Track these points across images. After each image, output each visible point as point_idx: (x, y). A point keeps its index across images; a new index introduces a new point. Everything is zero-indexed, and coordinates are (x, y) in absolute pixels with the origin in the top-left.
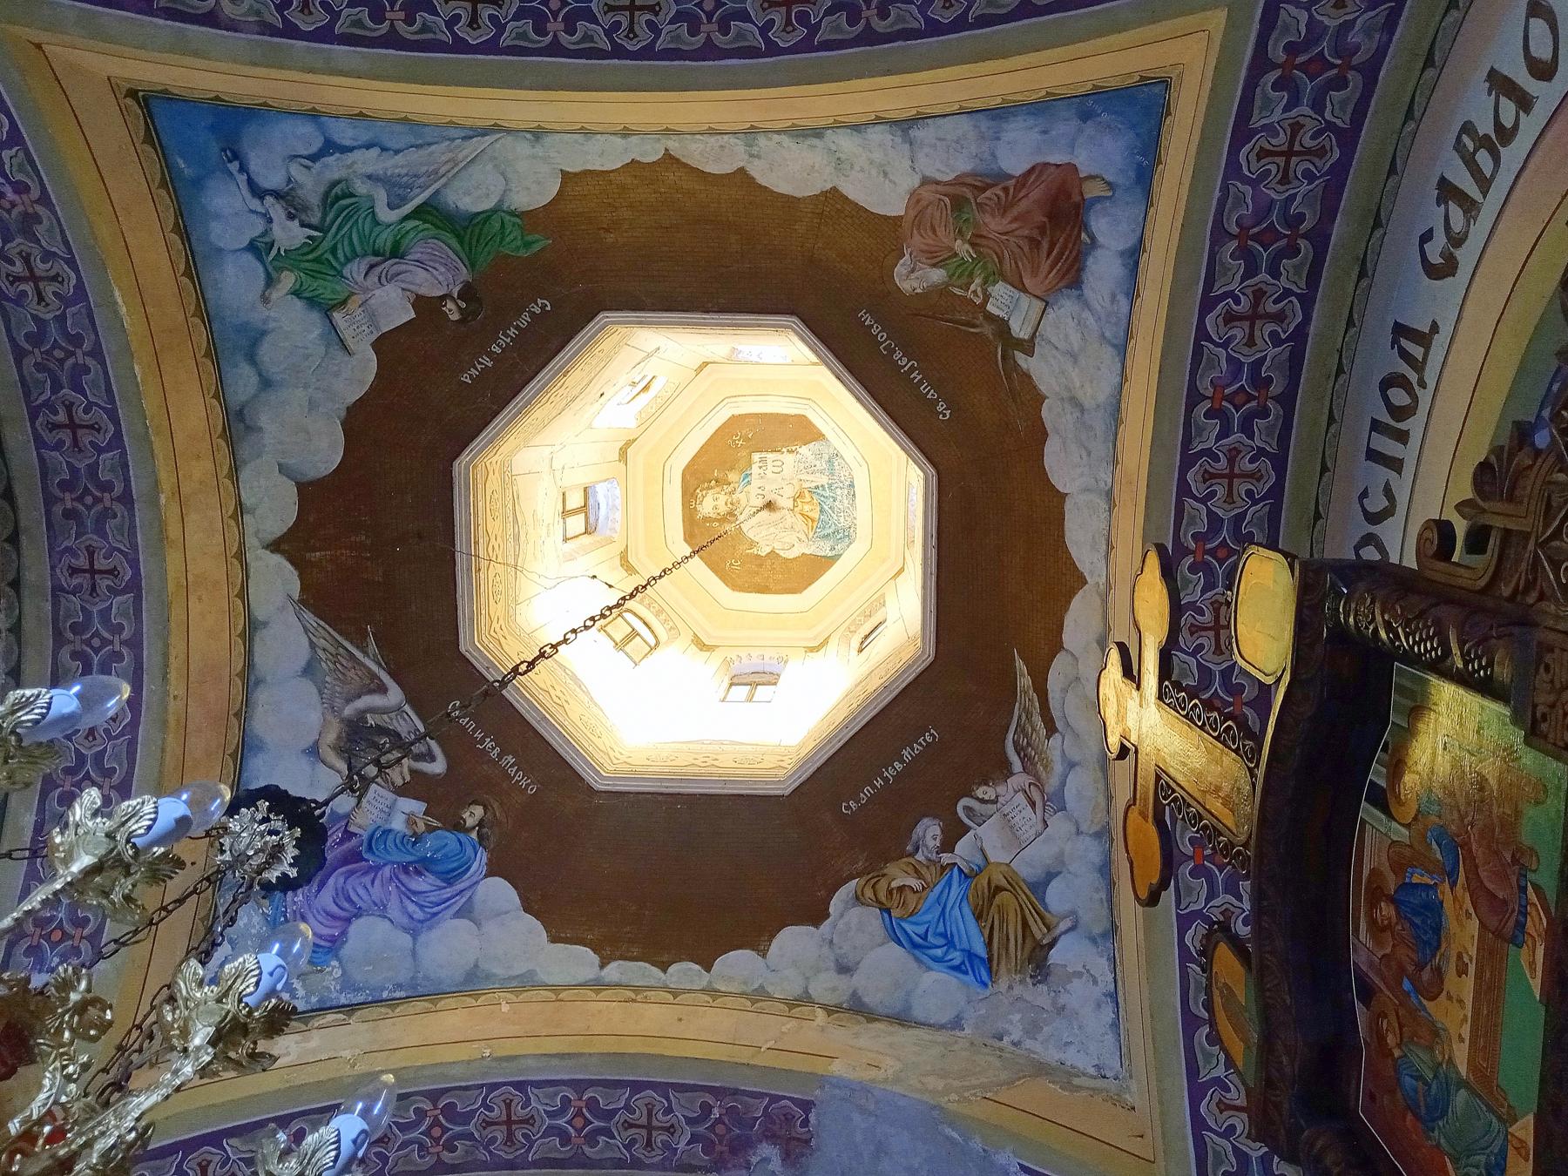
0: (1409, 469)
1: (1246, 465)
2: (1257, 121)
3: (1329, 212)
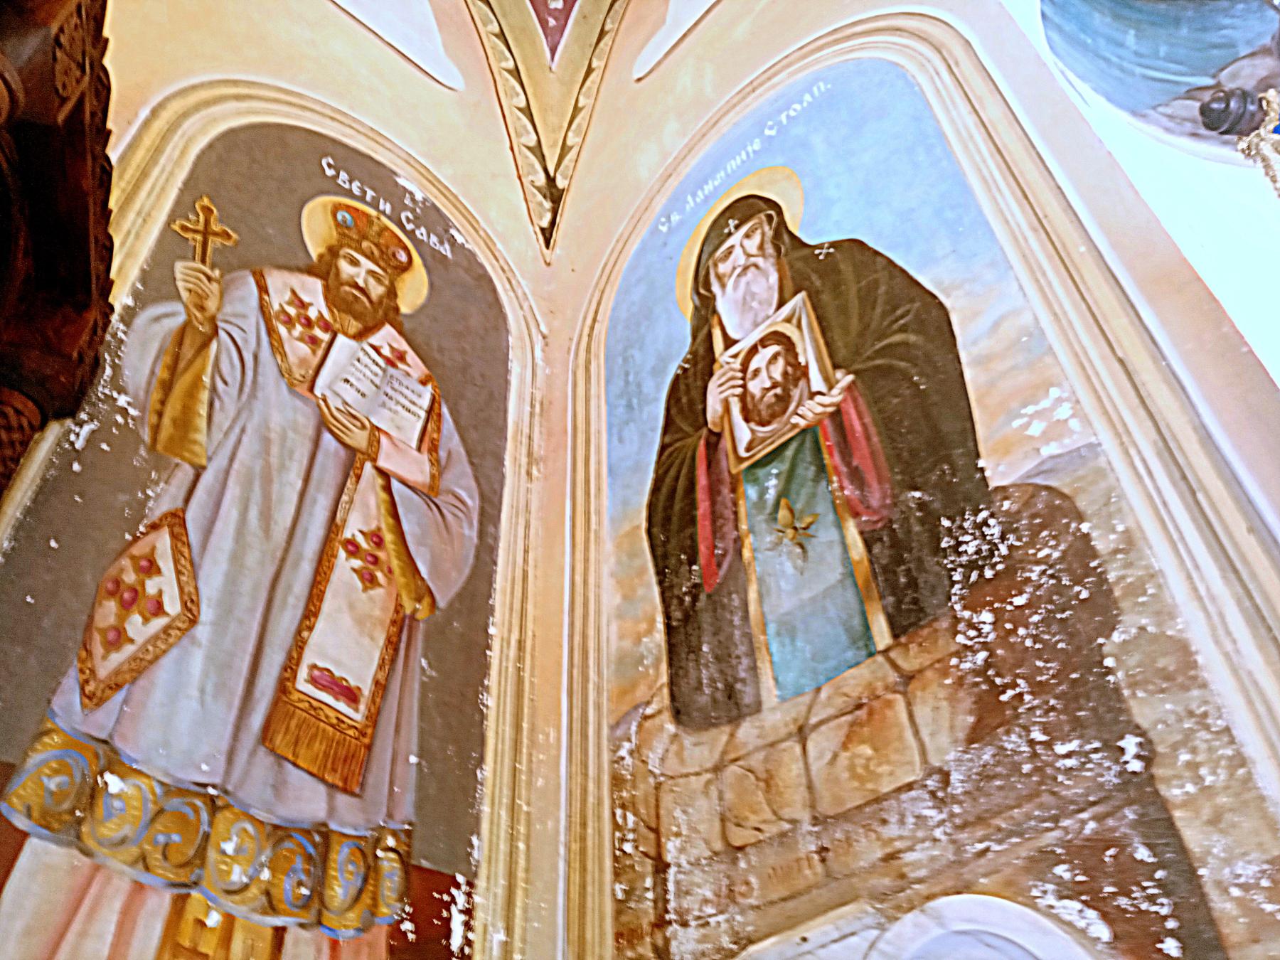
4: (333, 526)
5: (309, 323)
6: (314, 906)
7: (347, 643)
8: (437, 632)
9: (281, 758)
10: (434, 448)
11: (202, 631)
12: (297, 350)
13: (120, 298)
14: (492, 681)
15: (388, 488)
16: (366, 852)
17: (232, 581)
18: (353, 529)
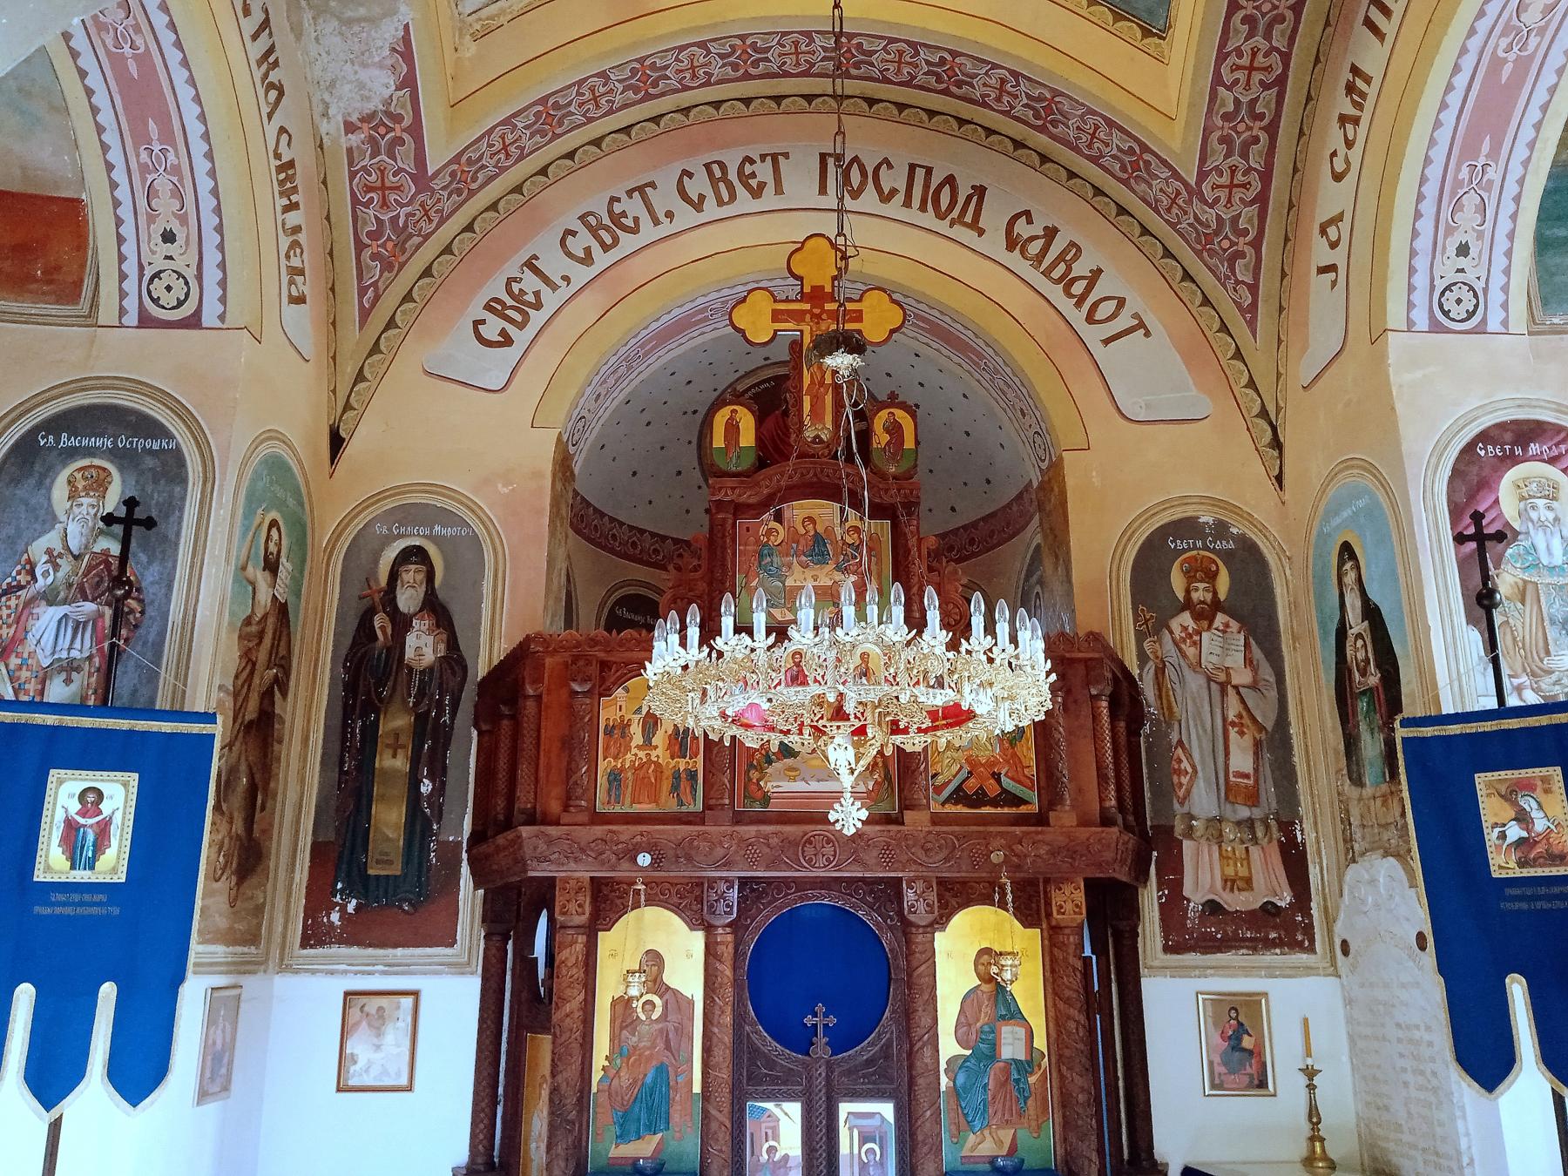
0: (904, 214)
3: (1053, 137)
4: (1224, 719)
5: (1190, 636)
6: (1255, 840)
7: (1242, 760)
8: (1271, 739)
11: (1200, 774)
12: (1191, 652)
13: (1136, 672)
15: (1238, 693)
16: (1265, 821)
18: (1231, 716)
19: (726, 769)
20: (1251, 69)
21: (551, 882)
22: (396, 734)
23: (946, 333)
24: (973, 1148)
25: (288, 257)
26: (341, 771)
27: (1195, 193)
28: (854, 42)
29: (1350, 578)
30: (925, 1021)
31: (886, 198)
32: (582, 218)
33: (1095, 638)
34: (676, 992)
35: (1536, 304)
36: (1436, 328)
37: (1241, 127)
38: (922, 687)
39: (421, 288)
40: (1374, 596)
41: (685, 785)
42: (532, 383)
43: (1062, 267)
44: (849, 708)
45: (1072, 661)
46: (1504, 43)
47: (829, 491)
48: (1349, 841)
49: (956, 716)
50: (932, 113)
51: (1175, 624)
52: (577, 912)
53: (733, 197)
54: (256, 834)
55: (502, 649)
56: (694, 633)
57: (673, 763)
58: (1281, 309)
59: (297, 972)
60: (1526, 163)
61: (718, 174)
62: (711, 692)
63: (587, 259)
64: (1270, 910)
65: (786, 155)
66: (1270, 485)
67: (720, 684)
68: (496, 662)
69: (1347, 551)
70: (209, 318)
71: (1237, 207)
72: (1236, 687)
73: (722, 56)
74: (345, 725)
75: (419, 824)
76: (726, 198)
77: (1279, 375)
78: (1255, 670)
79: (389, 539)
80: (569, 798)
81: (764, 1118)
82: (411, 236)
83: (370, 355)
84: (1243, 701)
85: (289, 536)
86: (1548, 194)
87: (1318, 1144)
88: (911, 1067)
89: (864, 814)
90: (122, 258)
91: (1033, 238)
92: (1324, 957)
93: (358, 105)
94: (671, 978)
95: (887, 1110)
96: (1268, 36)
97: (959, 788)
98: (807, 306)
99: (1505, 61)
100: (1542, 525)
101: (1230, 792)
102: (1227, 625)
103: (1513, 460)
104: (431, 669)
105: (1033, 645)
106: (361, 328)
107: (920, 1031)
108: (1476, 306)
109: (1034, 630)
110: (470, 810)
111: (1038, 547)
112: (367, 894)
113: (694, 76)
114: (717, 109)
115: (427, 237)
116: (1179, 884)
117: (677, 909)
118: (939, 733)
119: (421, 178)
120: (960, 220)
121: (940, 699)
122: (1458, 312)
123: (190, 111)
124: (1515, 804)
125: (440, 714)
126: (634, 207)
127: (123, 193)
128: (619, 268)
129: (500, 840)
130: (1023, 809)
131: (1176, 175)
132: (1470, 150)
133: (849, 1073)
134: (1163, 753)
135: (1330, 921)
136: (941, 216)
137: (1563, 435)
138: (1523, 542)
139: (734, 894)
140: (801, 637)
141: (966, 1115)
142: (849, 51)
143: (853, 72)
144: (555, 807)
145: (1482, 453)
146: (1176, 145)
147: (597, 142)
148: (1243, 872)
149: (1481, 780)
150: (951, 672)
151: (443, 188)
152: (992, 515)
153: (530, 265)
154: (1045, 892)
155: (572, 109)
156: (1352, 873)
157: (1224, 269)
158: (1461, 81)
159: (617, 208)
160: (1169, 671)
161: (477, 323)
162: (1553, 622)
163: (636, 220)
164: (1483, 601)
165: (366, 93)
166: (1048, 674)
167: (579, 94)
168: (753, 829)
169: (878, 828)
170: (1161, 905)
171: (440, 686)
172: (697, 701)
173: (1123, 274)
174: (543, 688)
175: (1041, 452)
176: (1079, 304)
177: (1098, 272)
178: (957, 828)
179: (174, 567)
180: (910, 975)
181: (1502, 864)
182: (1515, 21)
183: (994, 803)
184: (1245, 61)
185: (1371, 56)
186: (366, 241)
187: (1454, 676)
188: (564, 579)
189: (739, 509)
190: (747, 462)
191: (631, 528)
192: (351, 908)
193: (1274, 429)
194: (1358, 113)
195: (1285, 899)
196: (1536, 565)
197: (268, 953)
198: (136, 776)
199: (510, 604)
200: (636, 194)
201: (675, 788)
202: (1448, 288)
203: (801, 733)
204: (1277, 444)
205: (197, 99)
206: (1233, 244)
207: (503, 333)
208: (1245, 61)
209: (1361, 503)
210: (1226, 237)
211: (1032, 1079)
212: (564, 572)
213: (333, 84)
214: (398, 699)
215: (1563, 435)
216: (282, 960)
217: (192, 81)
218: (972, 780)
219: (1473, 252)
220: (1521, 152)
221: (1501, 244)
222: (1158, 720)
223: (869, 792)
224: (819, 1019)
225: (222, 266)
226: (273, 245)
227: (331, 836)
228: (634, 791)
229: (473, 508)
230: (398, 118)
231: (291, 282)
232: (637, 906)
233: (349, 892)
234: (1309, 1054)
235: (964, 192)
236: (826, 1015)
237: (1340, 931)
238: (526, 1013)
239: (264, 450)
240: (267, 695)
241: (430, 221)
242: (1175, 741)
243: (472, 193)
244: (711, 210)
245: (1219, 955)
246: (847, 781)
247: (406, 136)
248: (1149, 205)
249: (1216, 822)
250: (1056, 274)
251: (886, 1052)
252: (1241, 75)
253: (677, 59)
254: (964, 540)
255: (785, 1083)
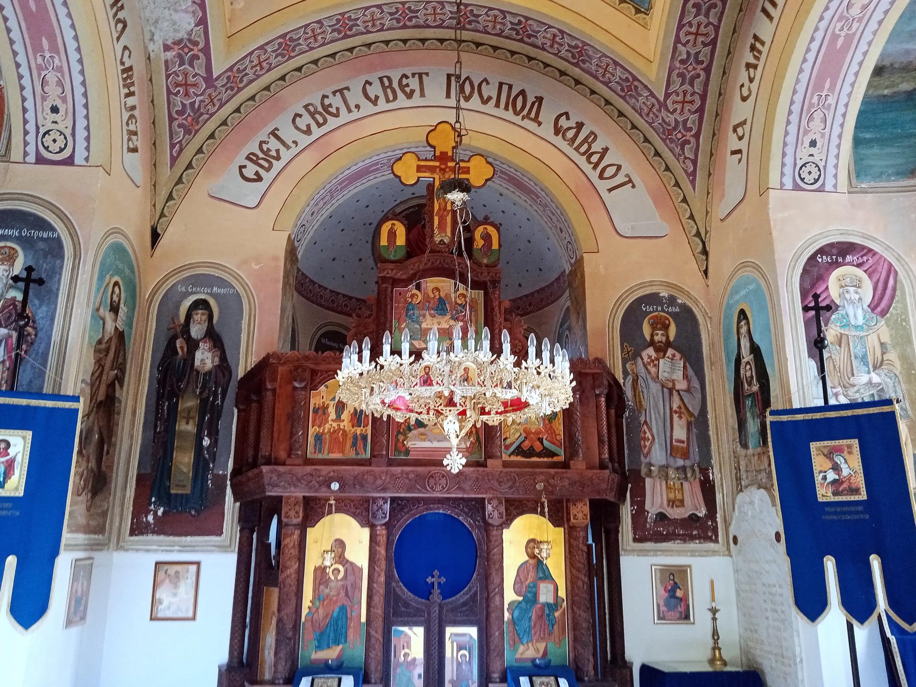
1: (498, 27)
2: (618, 68)
3: (583, 70)
4: (671, 409)
6: (686, 478)
7: (680, 433)
8: (697, 419)
9: (674, 457)
10: (687, 377)
12: (653, 370)
13: (621, 381)
14: (711, 428)
17: (657, 429)
18: (675, 407)
19: (384, 433)
20: (697, 34)
21: (279, 499)
22: (189, 410)
23: (517, 181)
24: (522, 654)
25: (128, 124)
26: (155, 430)
27: (663, 105)
28: (469, 8)
29: (744, 330)
30: (497, 581)
31: (485, 102)
32: (306, 107)
33: (599, 361)
34: (352, 564)
35: (853, 176)
36: (797, 188)
37: (690, 68)
38: (499, 388)
39: (208, 145)
40: (756, 340)
41: (360, 443)
42: (274, 203)
43: (585, 146)
44: (457, 399)
45: (586, 374)
46: (839, 25)
47: (450, 274)
48: (739, 479)
49: (518, 405)
50: (513, 53)
51: (645, 354)
52: (295, 516)
53: (395, 98)
54: (103, 468)
55: (253, 361)
56: (366, 354)
57: (353, 430)
58: (710, 174)
59: (127, 550)
60: (850, 95)
61: (387, 83)
62: (376, 389)
63: (308, 131)
64: (693, 518)
65: (427, 74)
66: (700, 275)
67: (381, 384)
68: (249, 369)
69: (742, 313)
70: (78, 160)
71: (687, 114)
72: (678, 391)
73: (391, 14)
74: (158, 405)
75: (202, 464)
76: (391, 98)
77: (707, 212)
78: (689, 381)
79: (186, 295)
80: (291, 449)
81: (403, 636)
82: (202, 114)
83: (177, 184)
84: (682, 399)
85: (126, 291)
86: (861, 113)
87: (717, 652)
88: (488, 606)
89: (464, 461)
90: (25, 122)
91: (569, 128)
92: (723, 545)
93: (171, 34)
94: (349, 555)
95: (473, 631)
96: (707, 15)
97: (519, 446)
98: (437, 164)
99: (839, 36)
100: (852, 302)
101: (672, 451)
102: (674, 355)
103: (836, 265)
104: (209, 373)
105: (563, 365)
106: (171, 168)
107: (493, 587)
108: (820, 176)
109: (564, 356)
110: (232, 456)
111: (568, 307)
112: (171, 505)
113: (373, 25)
114: (387, 45)
115: (212, 115)
116: (643, 502)
117: (354, 515)
118: (508, 415)
119: (209, 79)
120: (527, 116)
121: (510, 395)
122: (809, 179)
123: (69, 34)
124: (832, 459)
125: (215, 399)
126: (336, 101)
127: (26, 82)
128: (327, 137)
129: (250, 474)
130: (555, 459)
131: (652, 95)
132: (819, 86)
133: (454, 610)
134: (636, 427)
135: (727, 524)
136: (516, 113)
137: (865, 251)
138: (841, 312)
139: (387, 507)
140: (429, 358)
141: (518, 635)
142: (465, 14)
143: (468, 26)
144: (283, 455)
145: (820, 260)
146: (653, 77)
147: (315, 62)
148: (679, 496)
149: (814, 446)
150: (516, 380)
151: (222, 86)
152: (542, 289)
153: (274, 133)
154: (567, 508)
155: (301, 41)
156: (740, 497)
157: (678, 150)
158: (815, 46)
159: (327, 102)
160: (640, 381)
161: (241, 167)
162: (856, 357)
163: (338, 109)
164: (817, 345)
165: (176, 27)
166: (571, 382)
167: (305, 33)
168: (399, 469)
169: (472, 469)
170: (632, 515)
171: (216, 382)
172: (368, 394)
173: (621, 152)
174: (277, 385)
175: (571, 253)
176: (595, 168)
177: (606, 150)
178: (517, 470)
179: (56, 308)
180: (488, 554)
181: (824, 494)
182: (845, 13)
183: (539, 455)
184: (694, 30)
185: (765, 29)
186: (175, 116)
187: (800, 387)
188: (290, 321)
189: (395, 282)
190: (401, 254)
191: (332, 291)
192: (160, 512)
193: (704, 243)
194: (756, 62)
195: (702, 512)
196: (848, 325)
197: (109, 540)
198: (30, 433)
199: (259, 333)
200: (338, 94)
201: (354, 444)
202: (804, 165)
203: (428, 413)
204: (705, 252)
205: (73, 26)
206: (683, 136)
207: (257, 173)
208: (694, 30)
209: (751, 287)
210: (680, 132)
211: (557, 614)
212: (290, 317)
213: (157, 21)
214: (190, 389)
215: (865, 251)
216: (118, 543)
217: (69, 15)
218: (527, 442)
219: (819, 145)
220: (847, 89)
221: (835, 141)
222: (633, 409)
223: (467, 448)
224: (435, 579)
225: (87, 128)
226: (119, 117)
227: (149, 471)
228: (329, 447)
229: (238, 278)
230: (196, 44)
231: (129, 140)
232: (330, 513)
233: (158, 504)
234: (713, 600)
235: (531, 99)
236: (439, 577)
237: (732, 531)
238: (263, 576)
239: (111, 240)
240: (111, 386)
241: (214, 105)
242: (642, 422)
243: (240, 90)
244: (382, 105)
245: (664, 544)
246: (454, 442)
247: (201, 54)
248: (637, 111)
249: (664, 468)
250: (583, 149)
251: (473, 598)
252: (691, 37)
253: (364, 15)
254: (526, 301)
255: (415, 616)
